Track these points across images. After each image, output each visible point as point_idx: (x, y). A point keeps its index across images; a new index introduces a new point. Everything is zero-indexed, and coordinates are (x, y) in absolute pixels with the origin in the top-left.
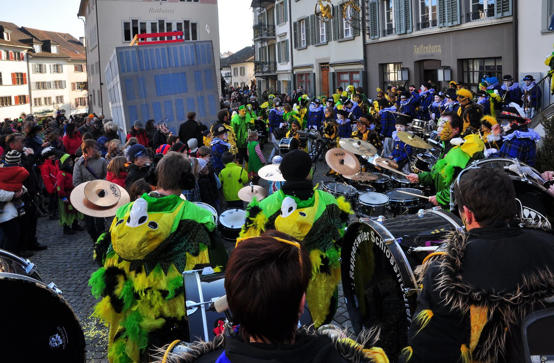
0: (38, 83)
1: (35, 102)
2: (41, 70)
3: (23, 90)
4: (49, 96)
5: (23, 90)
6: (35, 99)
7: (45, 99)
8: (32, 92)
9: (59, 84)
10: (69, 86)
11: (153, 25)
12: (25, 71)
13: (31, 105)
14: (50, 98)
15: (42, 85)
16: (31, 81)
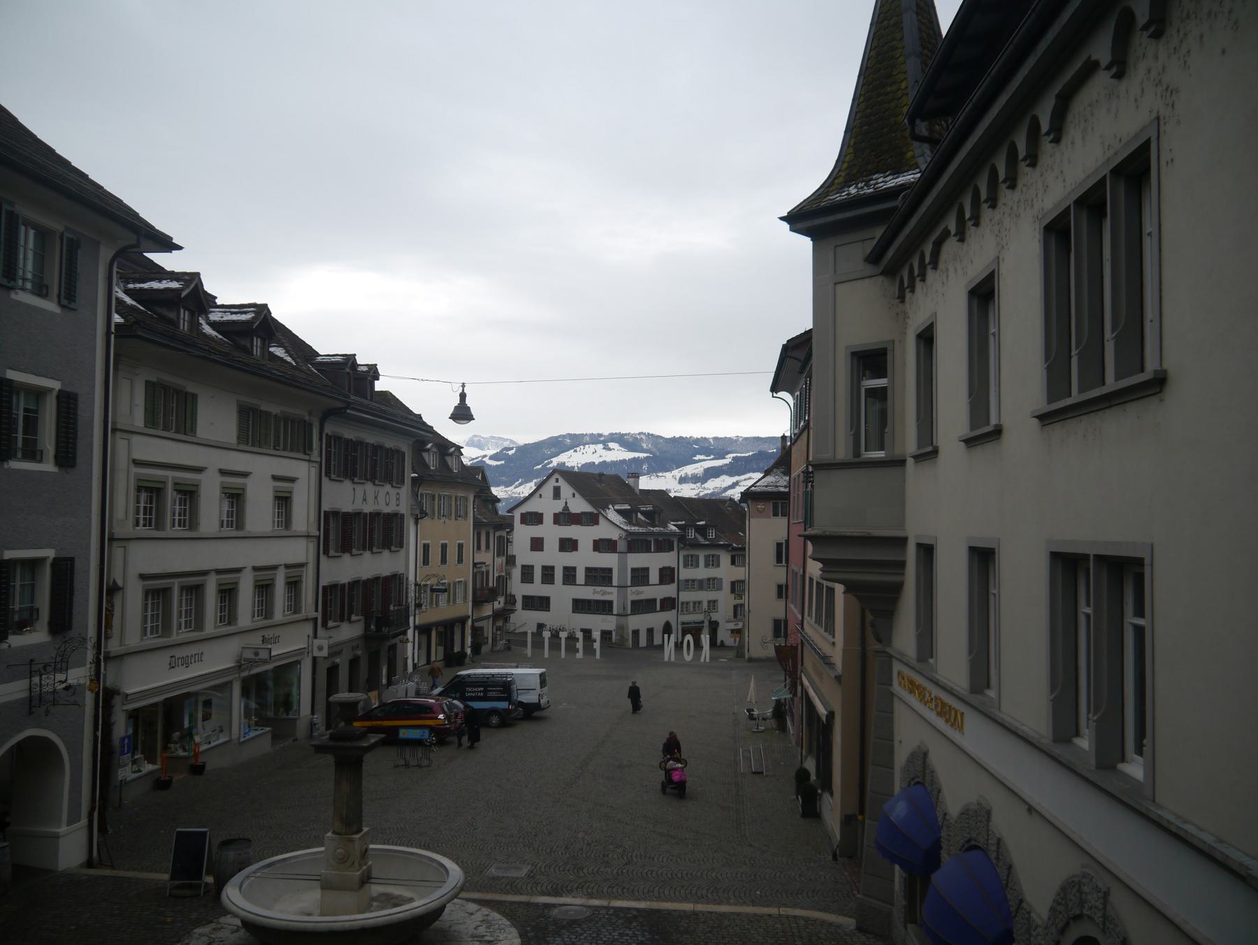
0: (687, 581)
1: (682, 608)
2: (691, 562)
3: (669, 590)
4: (700, 600)
5: (669, 590)
6: (682, 603)
7: (695, 603)
8: (680, 593)
9: (713, 584)
10: (727, 587)
12: (674, 565)
13: (678, 611)
14: (700, 602)
15: (691, 584)
16: (680, 578)
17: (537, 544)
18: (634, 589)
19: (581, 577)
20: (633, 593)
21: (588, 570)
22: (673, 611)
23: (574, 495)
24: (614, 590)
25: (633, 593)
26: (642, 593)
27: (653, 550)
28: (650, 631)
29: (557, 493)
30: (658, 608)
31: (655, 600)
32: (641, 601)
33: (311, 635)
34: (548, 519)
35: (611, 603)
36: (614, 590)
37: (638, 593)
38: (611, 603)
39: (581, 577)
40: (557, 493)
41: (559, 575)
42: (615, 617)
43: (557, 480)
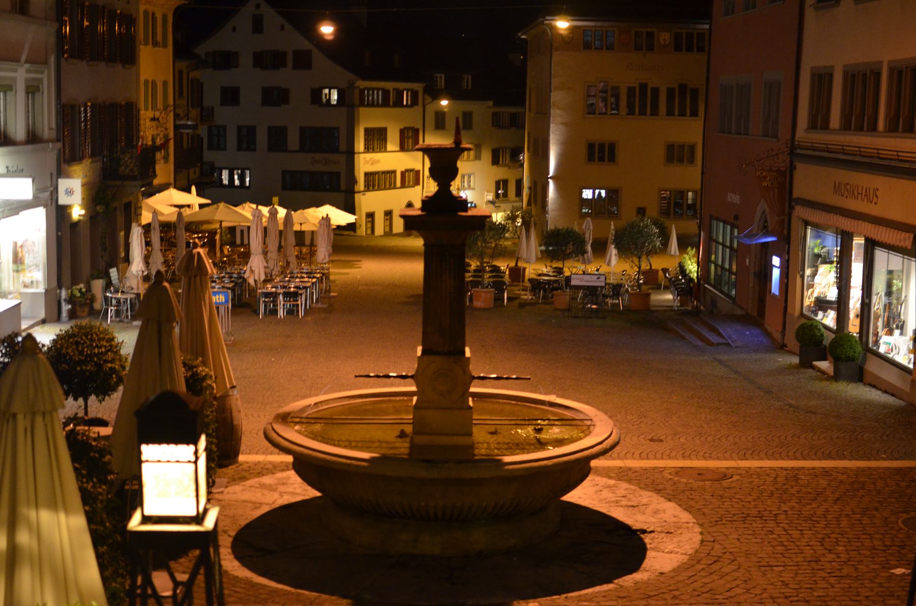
11: (631, 91)
17: (231, 96)
18: (369, 156)
19: (293, 140)
20: (366, 162)
21: (303, 130)
22: (417, 187)
23: (283, 28)
24: (342, 158)
25: (366, 162)
26: (378, 161)
27: (391, 103)
28: (388, 214)
29: (258, 25)
30: (398, 184)
31: (394, 172)
32: (377, 173)
33: (55, 173)
34: (246, 60)
35: (338, 174)
36: (342, 158)
37: (374, 162)
38: (338, 174)
39: (293, 140)
40: (258, 25)
41: (262, 138)
42: (343, 194)
43: (258, 6)
